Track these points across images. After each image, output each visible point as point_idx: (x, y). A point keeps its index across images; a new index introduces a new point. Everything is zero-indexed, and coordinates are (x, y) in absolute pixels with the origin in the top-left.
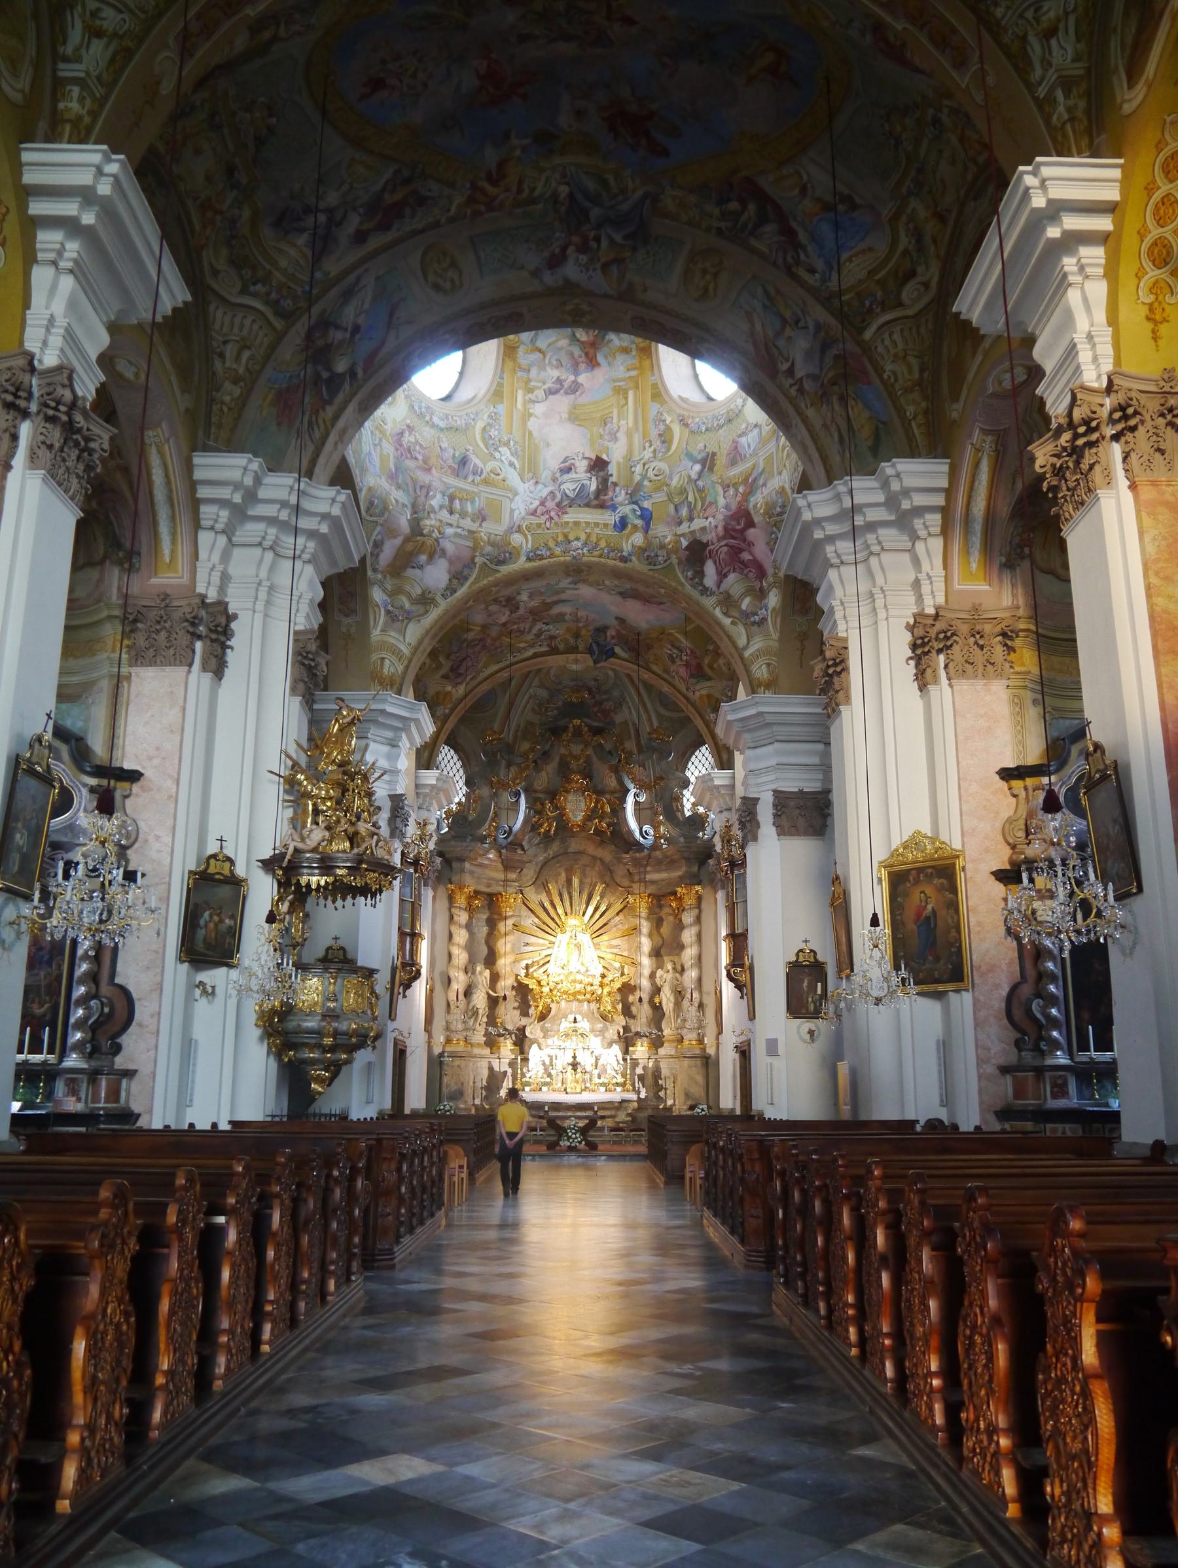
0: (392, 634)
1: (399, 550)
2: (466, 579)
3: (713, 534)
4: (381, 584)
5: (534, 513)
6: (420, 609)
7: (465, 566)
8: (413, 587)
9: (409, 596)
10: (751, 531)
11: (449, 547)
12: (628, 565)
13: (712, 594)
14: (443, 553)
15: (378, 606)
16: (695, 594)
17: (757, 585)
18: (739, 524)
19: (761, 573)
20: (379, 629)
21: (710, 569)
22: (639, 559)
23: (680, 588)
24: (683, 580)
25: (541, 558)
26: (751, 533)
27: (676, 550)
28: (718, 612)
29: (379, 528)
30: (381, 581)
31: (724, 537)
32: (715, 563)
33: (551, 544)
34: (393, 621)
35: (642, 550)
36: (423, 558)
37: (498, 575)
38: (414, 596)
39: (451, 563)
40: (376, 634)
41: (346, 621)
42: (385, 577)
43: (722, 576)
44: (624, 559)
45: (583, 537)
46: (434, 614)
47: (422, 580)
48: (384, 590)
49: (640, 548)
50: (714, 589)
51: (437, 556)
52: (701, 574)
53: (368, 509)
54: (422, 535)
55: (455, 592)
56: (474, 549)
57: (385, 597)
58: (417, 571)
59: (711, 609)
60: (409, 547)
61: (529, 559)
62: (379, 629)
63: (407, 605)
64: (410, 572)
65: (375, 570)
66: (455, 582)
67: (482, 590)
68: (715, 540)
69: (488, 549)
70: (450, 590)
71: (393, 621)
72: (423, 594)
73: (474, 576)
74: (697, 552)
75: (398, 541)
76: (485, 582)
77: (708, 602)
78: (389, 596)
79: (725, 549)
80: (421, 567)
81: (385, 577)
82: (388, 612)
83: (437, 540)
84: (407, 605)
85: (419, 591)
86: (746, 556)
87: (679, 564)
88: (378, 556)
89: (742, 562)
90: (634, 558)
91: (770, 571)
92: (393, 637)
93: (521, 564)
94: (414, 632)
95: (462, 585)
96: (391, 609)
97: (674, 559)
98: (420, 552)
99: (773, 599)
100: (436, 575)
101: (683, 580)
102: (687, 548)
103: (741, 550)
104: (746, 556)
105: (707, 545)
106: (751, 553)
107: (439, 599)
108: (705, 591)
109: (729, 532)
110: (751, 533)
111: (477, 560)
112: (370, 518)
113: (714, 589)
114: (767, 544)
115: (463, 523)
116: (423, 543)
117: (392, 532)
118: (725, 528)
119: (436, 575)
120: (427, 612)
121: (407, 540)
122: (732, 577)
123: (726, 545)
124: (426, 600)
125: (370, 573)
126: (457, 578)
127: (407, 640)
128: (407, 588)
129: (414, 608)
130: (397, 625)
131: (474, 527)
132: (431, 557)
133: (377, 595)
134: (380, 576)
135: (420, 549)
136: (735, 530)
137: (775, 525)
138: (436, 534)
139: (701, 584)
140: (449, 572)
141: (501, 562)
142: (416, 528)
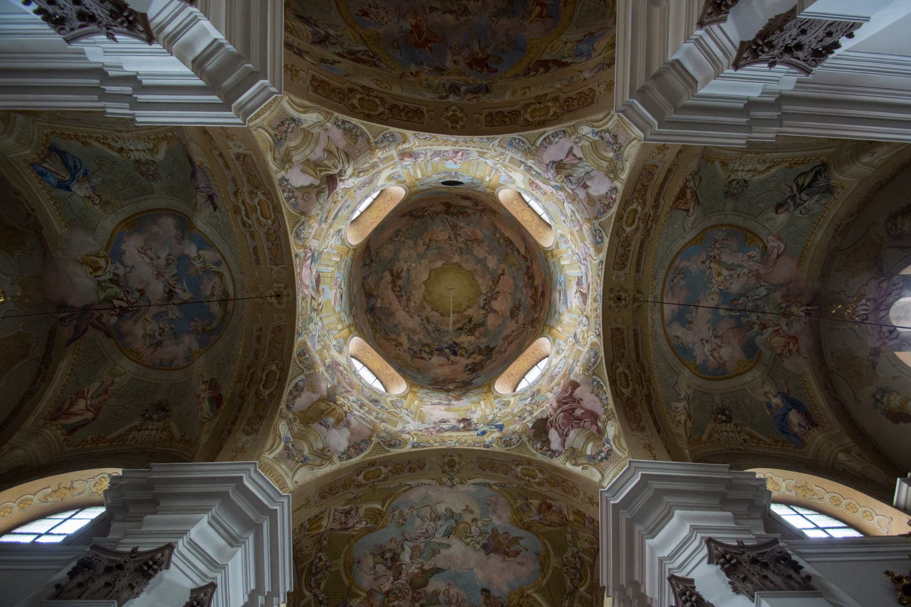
0: (284, 467)
1: (314, 403)
2: (362, 451)
3: (550, 409)
4: (290, 423)
5: (421, 431)
6: (318, 462)
7: (363, 441)
8: (316, 440)
9: (311, 446)
10: (578, 390)
11: (354, 423)
12: (490, 449)
13: (560, 453)
14: (348, 425)
15: (280, 437)
16: (546, 459)
17: (595, 428)
18: (567, 392)
19: (594, 417)
20: (272, 455)
21: (554, 435)
22: (497, 444)
23: (533, 457)
24: (534, 452)
25: (424, 447)
26: (578, 392)
27: (525, 432)
28: (568, 466)
29: (302, 377)
30: (290, 420)
31: (559, 407)
32: (556, 429)
33: (431, 442)
34: (289, 457)
35: (501, 438)
36: (331, 420)
37: (389, 454)
38: (315, 448)
39: (352, 434)
40: (269, 456)
41: (245, 438)
42: (295, 419)
43: (564, 436)
44: (485, 446)
45: (455, 440)
46: (327, 469)
47: (325, 438)
48: (291, 430)
49: (497, 438)
50: (561, 449)
51: (342, 424)
52: (547, 442)
53: (299, 355)
54: (335, 403)
55: (351, 458)
56: (373, 431)
57: (289, 436)
58: (323, 428)
59: (562, 466)
60: (323, 406)
61: (413, 447)
62: (272, 455)
63: (306, 452)
64: (316, 426)
65: (288, 407)
66: (352, 450)
67: (372, 464)
68: (552, 414)
69: (384, 434)
70: (347, 455)
71: (289, 457)
72: (324, 449)
73: (369, 450)
74: (541, 428)
75: (315, 397)
76: (377, 457)
77: (558, 462)
78: (293, 437)
79: (562, 415)
80: (327, 427)
81: (295, 419)
82: (286, 448)
83: (346, 413)
84: (306, 452)
85: (320, 446)
86: (579, 412)
87: (528, 441)
88: (295, 398)
89: (578, 419)
90: (494, 445)
91: (600, 411)
92: (282, 469)
93: (408, 448)
94: (304, 475)
95: (358, 454)
96: (290, 445)
97: (525, 439)
98: (329, 414)
99: (612, 430)
100: (339, 439)
101: (534, 452)
102: (532, 428)
103: (573, 410)
104: (579, 412)
105: (547, 418)
106: (582, 408)
107: (335, 459)
108: (554, 454)
109: (560, 402)
110: (578, 392)
111: (373, 439)
112: (298, 363)
113: (561, 449)
114: (592, 392)
115: (367, 415)
116: (334, 409)
117: (314, 388)
118: (558, 402)
119: (339, 439)
120: (322, 465)
121: (322, 400)
122: (572, 433)
123: (562, 411)
124: (324, 455)
125: (283, 406)
126: (356, 447)
127: (296, 478)
128: (312, 439)
129: (311, 457)
130: (290, 462)
131: (377, 421)
132: (338, 421)
133: (283, 428)
134: (291, 416)
135: (330, 413)
136: (565, 398)
137: (594, 374)
138: (346, 408)
139: (550, 450)
140: (349, 440)
141: (391, 446)
142: (331, 397)
